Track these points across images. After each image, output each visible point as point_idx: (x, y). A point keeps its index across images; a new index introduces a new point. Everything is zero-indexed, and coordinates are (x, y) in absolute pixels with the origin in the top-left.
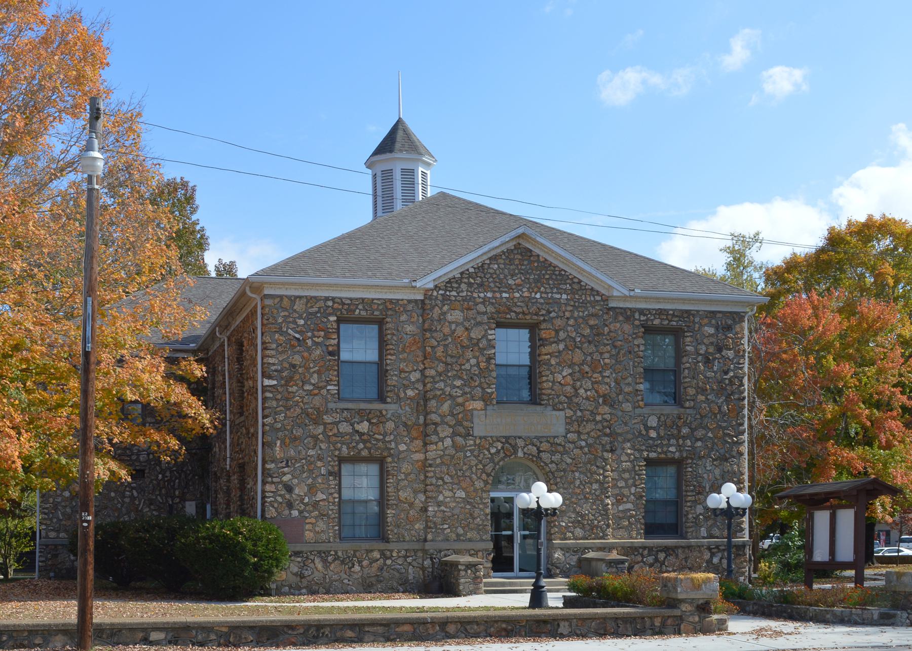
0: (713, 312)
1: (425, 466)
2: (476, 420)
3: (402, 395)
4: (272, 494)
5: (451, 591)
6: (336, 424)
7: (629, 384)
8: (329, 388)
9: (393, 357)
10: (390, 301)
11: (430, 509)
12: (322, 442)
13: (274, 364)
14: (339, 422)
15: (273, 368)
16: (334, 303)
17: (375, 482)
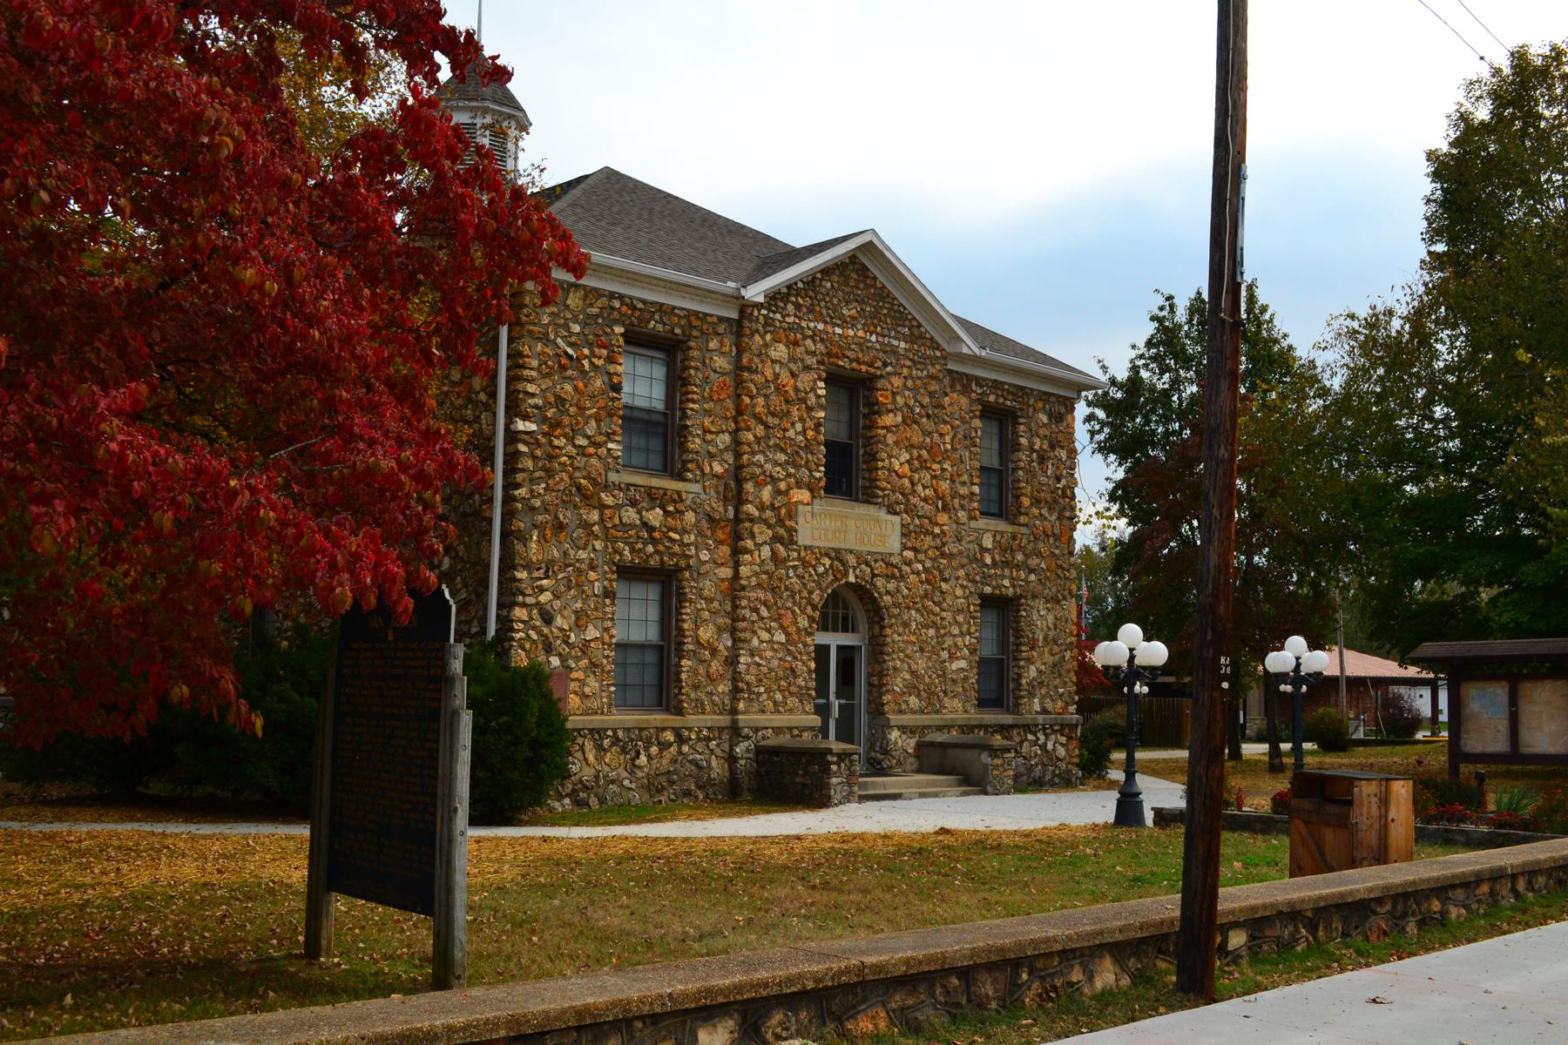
0: (1046, 393)
1: (733, 589)
2: (801, 520)
3: (707, 470)
4: (521, 626)
5: (814, 797)
6: (618, 507)
7: (964, 483)
8: (610, 445)
9: (695, 406)
10: (696, 313)
11: (742, 660)
12: (597, 537)
13: (533, 395)
14: (622, 506)
15: (532, 401)
16: (623, 304)
17: (654, 613)
